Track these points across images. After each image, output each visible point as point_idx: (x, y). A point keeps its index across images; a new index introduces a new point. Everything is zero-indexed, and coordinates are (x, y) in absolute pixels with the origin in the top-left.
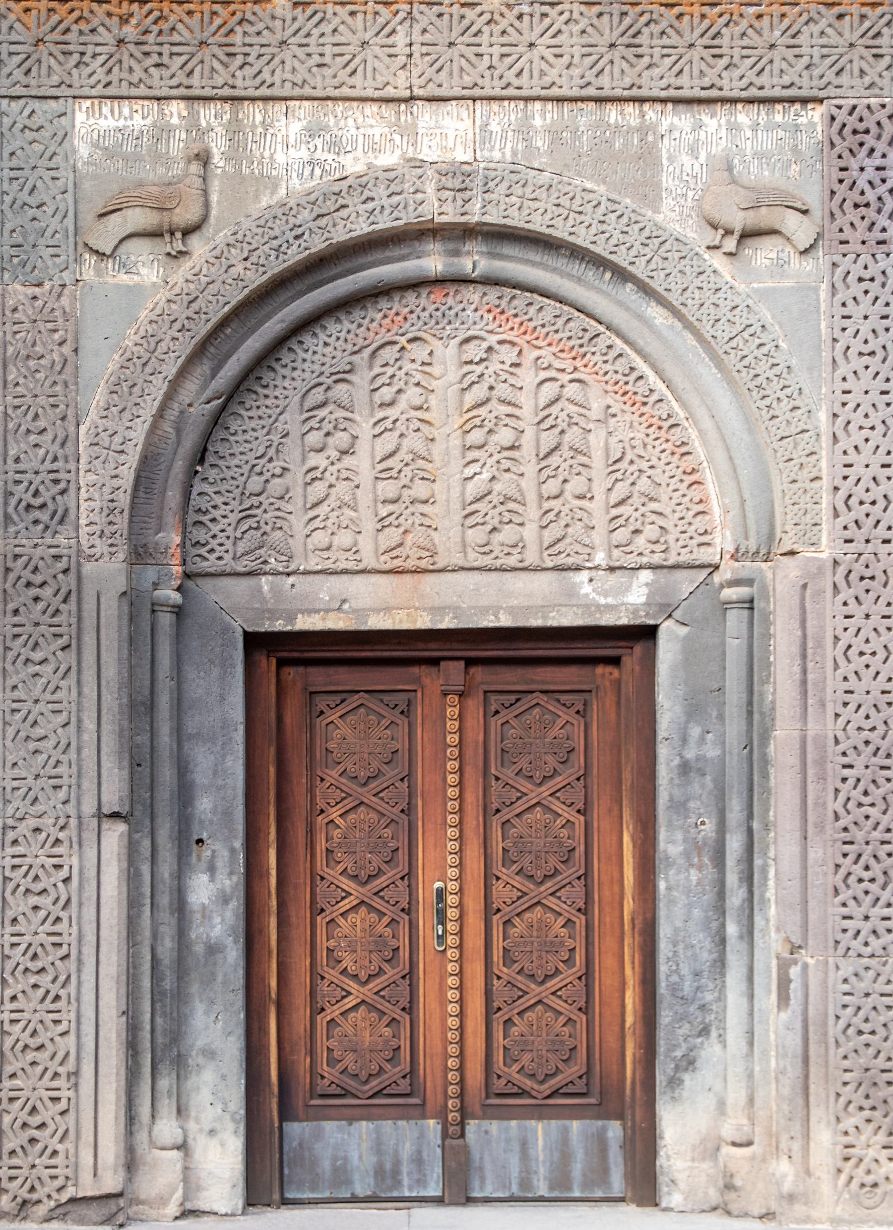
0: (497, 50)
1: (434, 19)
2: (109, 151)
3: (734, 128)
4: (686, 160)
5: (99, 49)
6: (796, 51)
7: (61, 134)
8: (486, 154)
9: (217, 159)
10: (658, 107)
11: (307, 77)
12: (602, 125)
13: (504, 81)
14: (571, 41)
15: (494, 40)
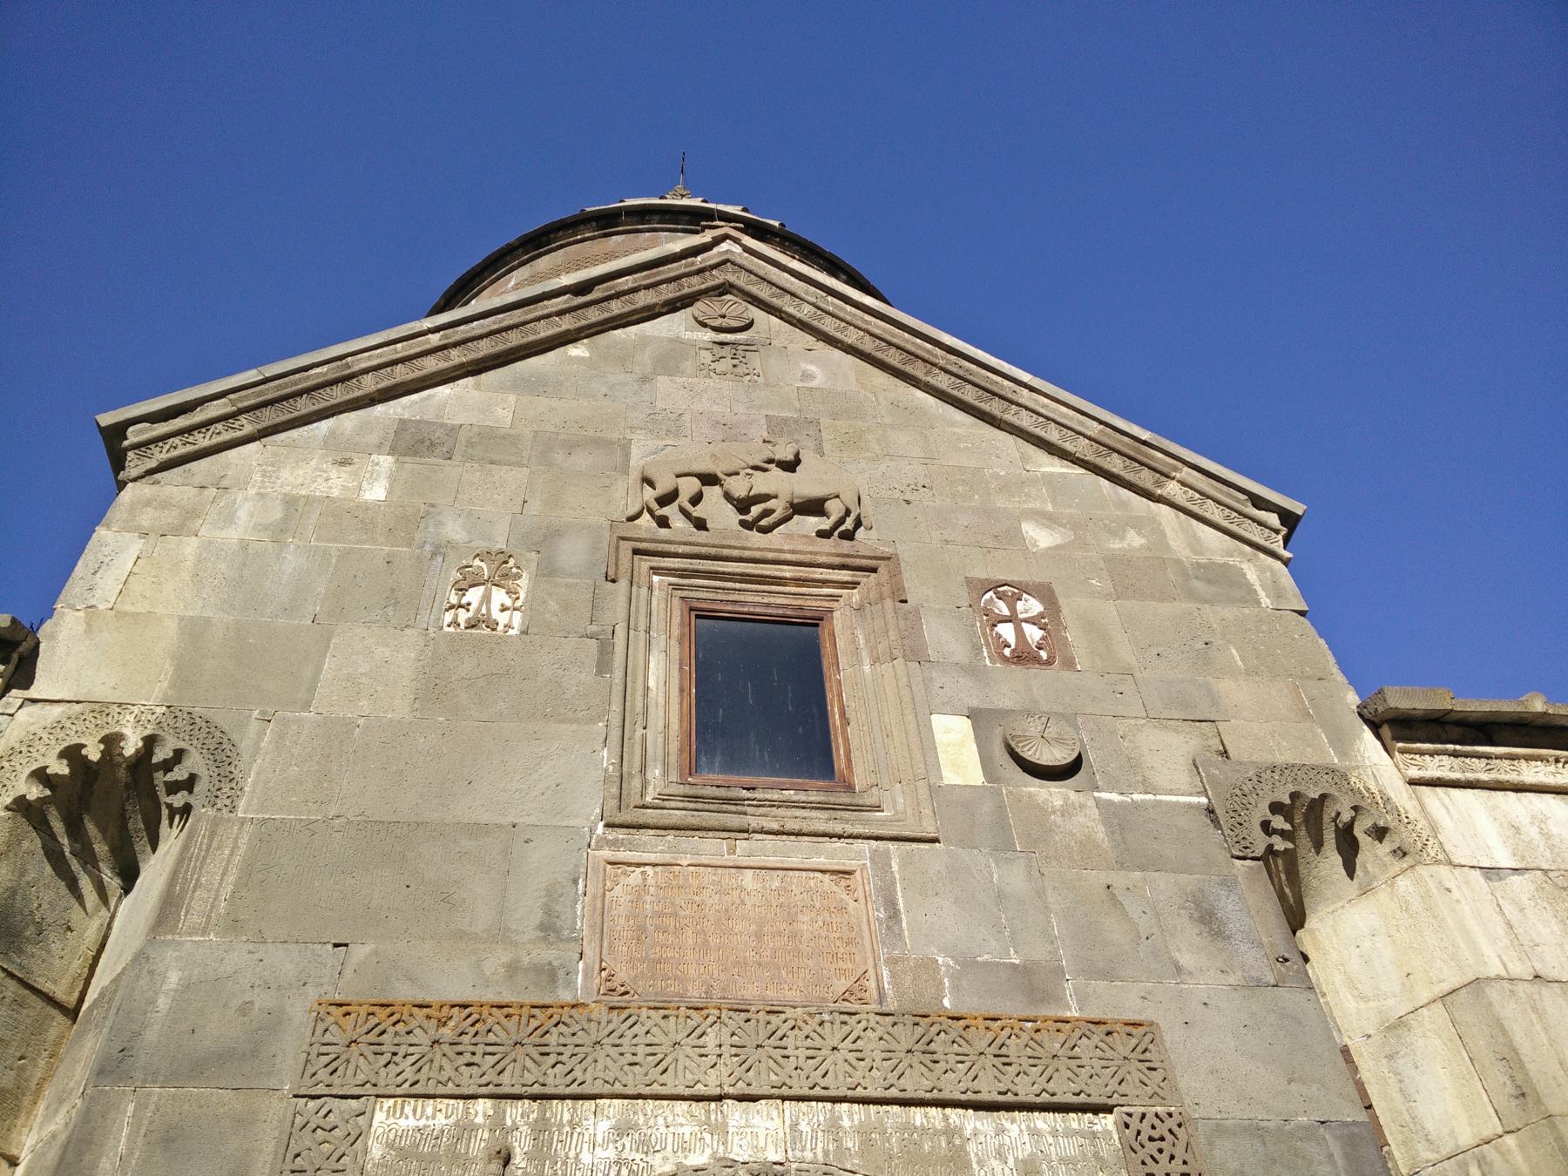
0: (802, 1053)
1: (742, 1024)
2: (403, 1151)
3: (1035, 1133)
4: (995, 1163)
5: (411, 1050)
6: (1078, 1062)
7: (354, 1134)
8: (799, 1154)
9: (518, 1160)
10: (960, 1111)
11: (619, 1075)
12: (908, 1127)
13: (811, 1082)
14: (870, 1044)
15: (799, 1044)
